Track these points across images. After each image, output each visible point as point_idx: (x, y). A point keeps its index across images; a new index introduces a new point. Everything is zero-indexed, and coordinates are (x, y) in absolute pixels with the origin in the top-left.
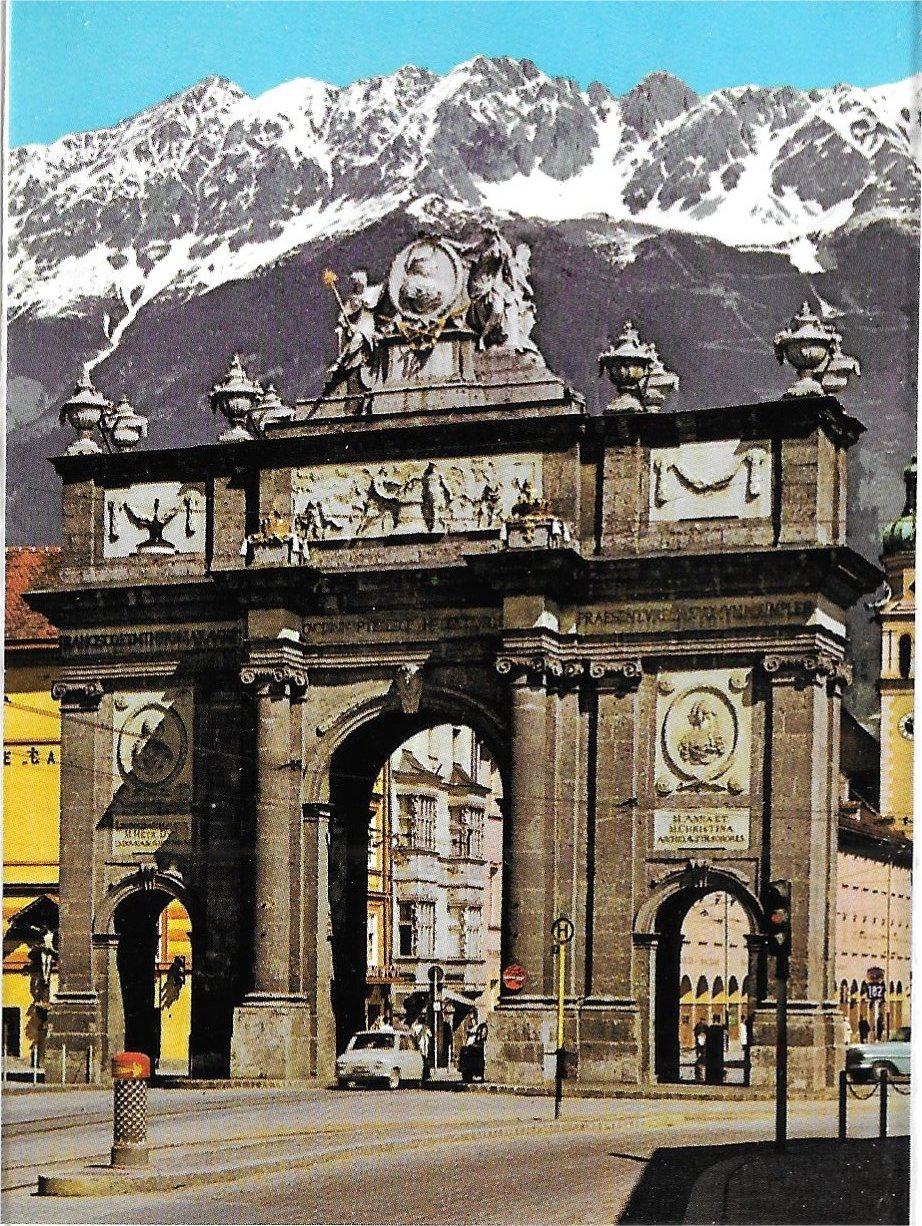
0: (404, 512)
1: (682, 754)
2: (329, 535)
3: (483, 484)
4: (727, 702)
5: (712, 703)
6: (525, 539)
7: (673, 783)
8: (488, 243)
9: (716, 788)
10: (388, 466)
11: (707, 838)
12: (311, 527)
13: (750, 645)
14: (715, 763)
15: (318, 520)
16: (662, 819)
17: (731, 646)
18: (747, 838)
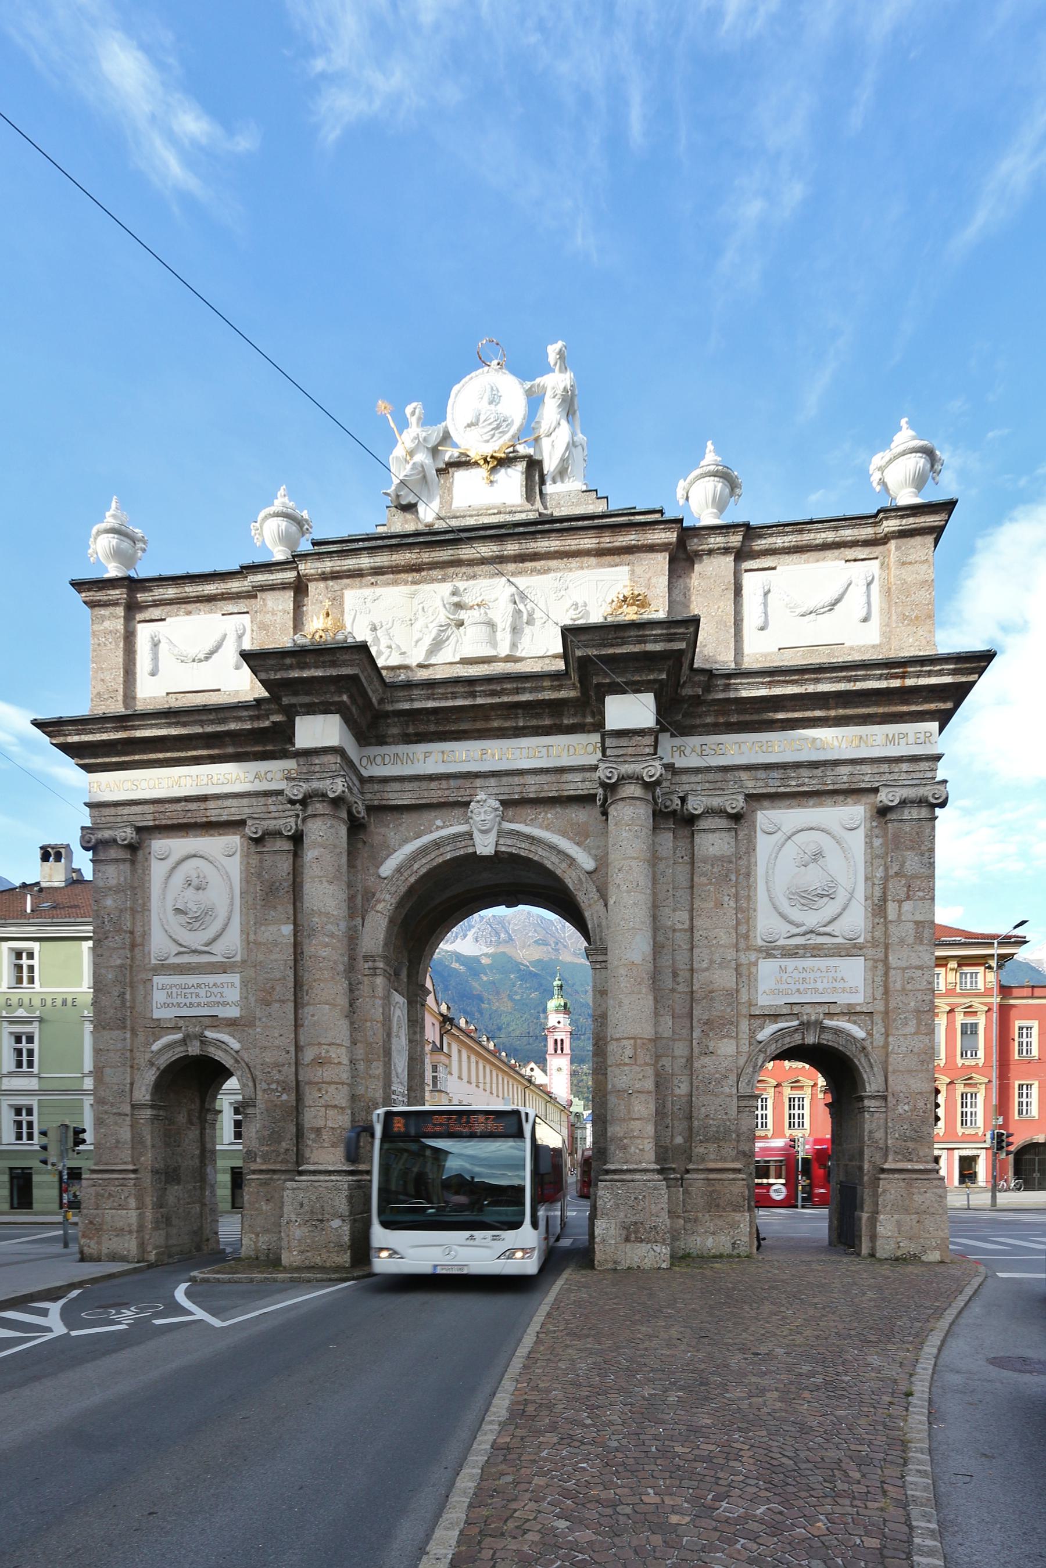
11: (816, 990)
14: (830, 909)
18: (861, 989)
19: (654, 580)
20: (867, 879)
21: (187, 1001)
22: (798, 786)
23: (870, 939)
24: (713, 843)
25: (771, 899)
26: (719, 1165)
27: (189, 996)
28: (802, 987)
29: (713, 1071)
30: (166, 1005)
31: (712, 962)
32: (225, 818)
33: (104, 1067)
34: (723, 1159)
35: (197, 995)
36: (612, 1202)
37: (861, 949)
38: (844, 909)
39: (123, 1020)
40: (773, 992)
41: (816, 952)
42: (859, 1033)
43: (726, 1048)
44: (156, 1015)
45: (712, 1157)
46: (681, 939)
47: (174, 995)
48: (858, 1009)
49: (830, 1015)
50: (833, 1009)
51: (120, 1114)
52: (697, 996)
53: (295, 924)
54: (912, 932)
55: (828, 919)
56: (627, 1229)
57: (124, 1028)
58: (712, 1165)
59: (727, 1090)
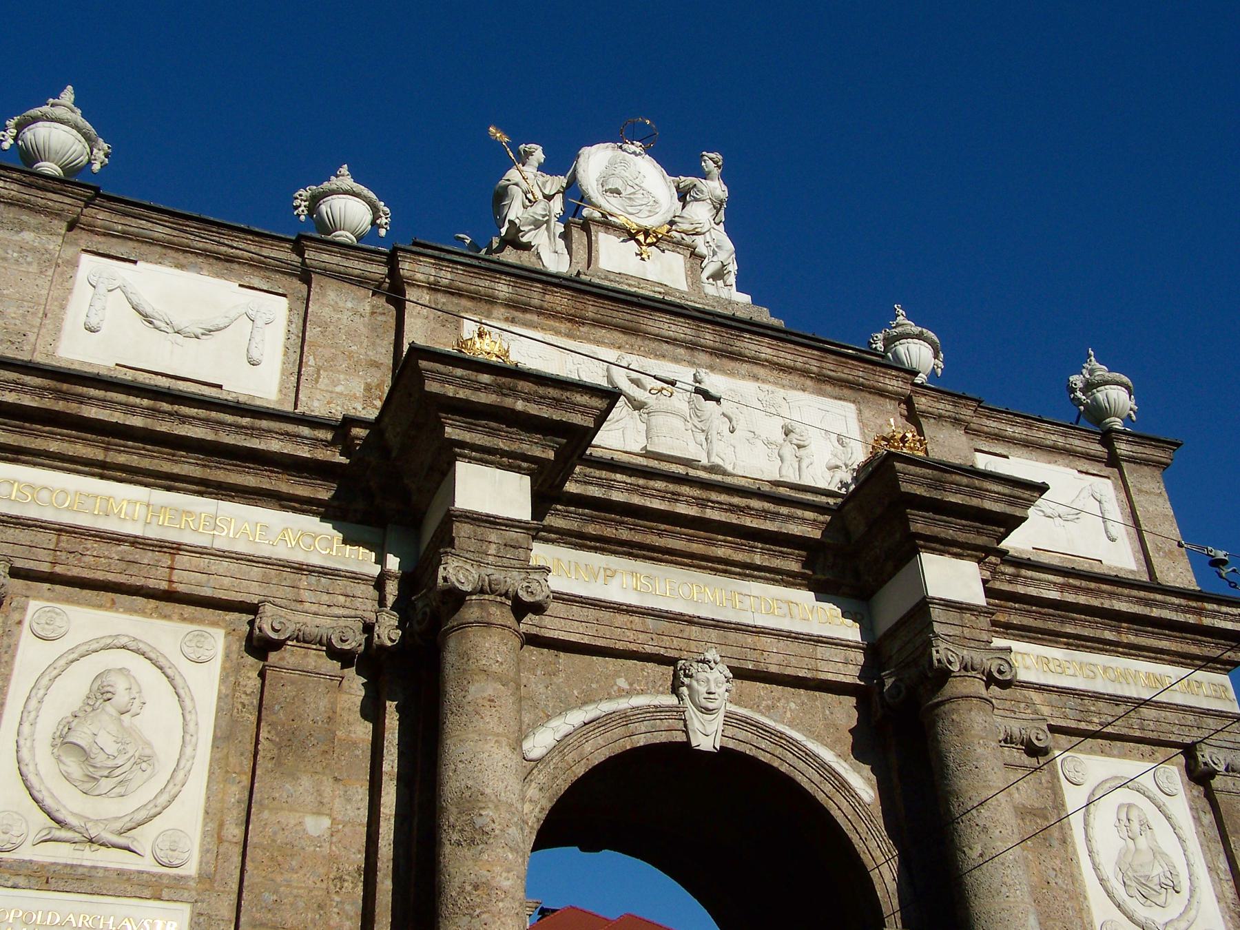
25: (1101, 880)
32: (208, 592)
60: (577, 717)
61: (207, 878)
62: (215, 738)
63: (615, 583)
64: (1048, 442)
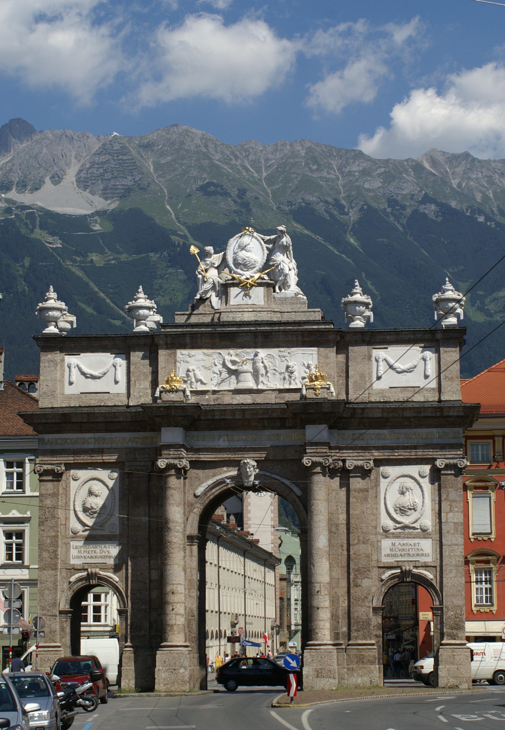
0: (242, 377)
1: (395, 510)
2: (201, 388)
3: (285, 364)
4: (419, 484)
5: (409, 483)
6: (316, 394)
7: (390, 524)
8: (280, 237)
9: (414, 528)
10: (232, 351)
11: (409, 555)
12: (189, 382)
13: (430, 453)
15: (193, 380)
16: (386, 544)
17: (420, 453)
18: (431, 554)
19: (329, 355)
20: (432, 500)
21: (90, 555)
22: (398, 456)
23: (434, 530)
24: (356, 483)
26: (364, 642)
27: (91, 552)
28: (403, 553)
29: (360, 595)
30: (78, 557)
31: (359, 540)
33: (44, 590)
34: (365, 639)
35: (95, 552)
36: (310, 659)
37: (430, 535)
38: (422, 515)
39: (56, 565)
40: (388, 555)
41: (409, 536)
42: (429, 575)
43: (366, 583)
44: (72, 562)
45: (360, 637)
46: (343, 528)
47: (82, 552)
48: (429, 564)
49: (416, 567)
50: (417, 564)
51: (52, 616)
52: (352, 557)
53: (149, 517)
54: (453, 527)
55: (414, 520)
56: (317, 671)
57: (56, 569)
58: (360, 642)
59: (367, 604)
60: (210, 482)
61: (121, 534)
62: (120, 499)
63: (221, 440)
64: (406, 339)
